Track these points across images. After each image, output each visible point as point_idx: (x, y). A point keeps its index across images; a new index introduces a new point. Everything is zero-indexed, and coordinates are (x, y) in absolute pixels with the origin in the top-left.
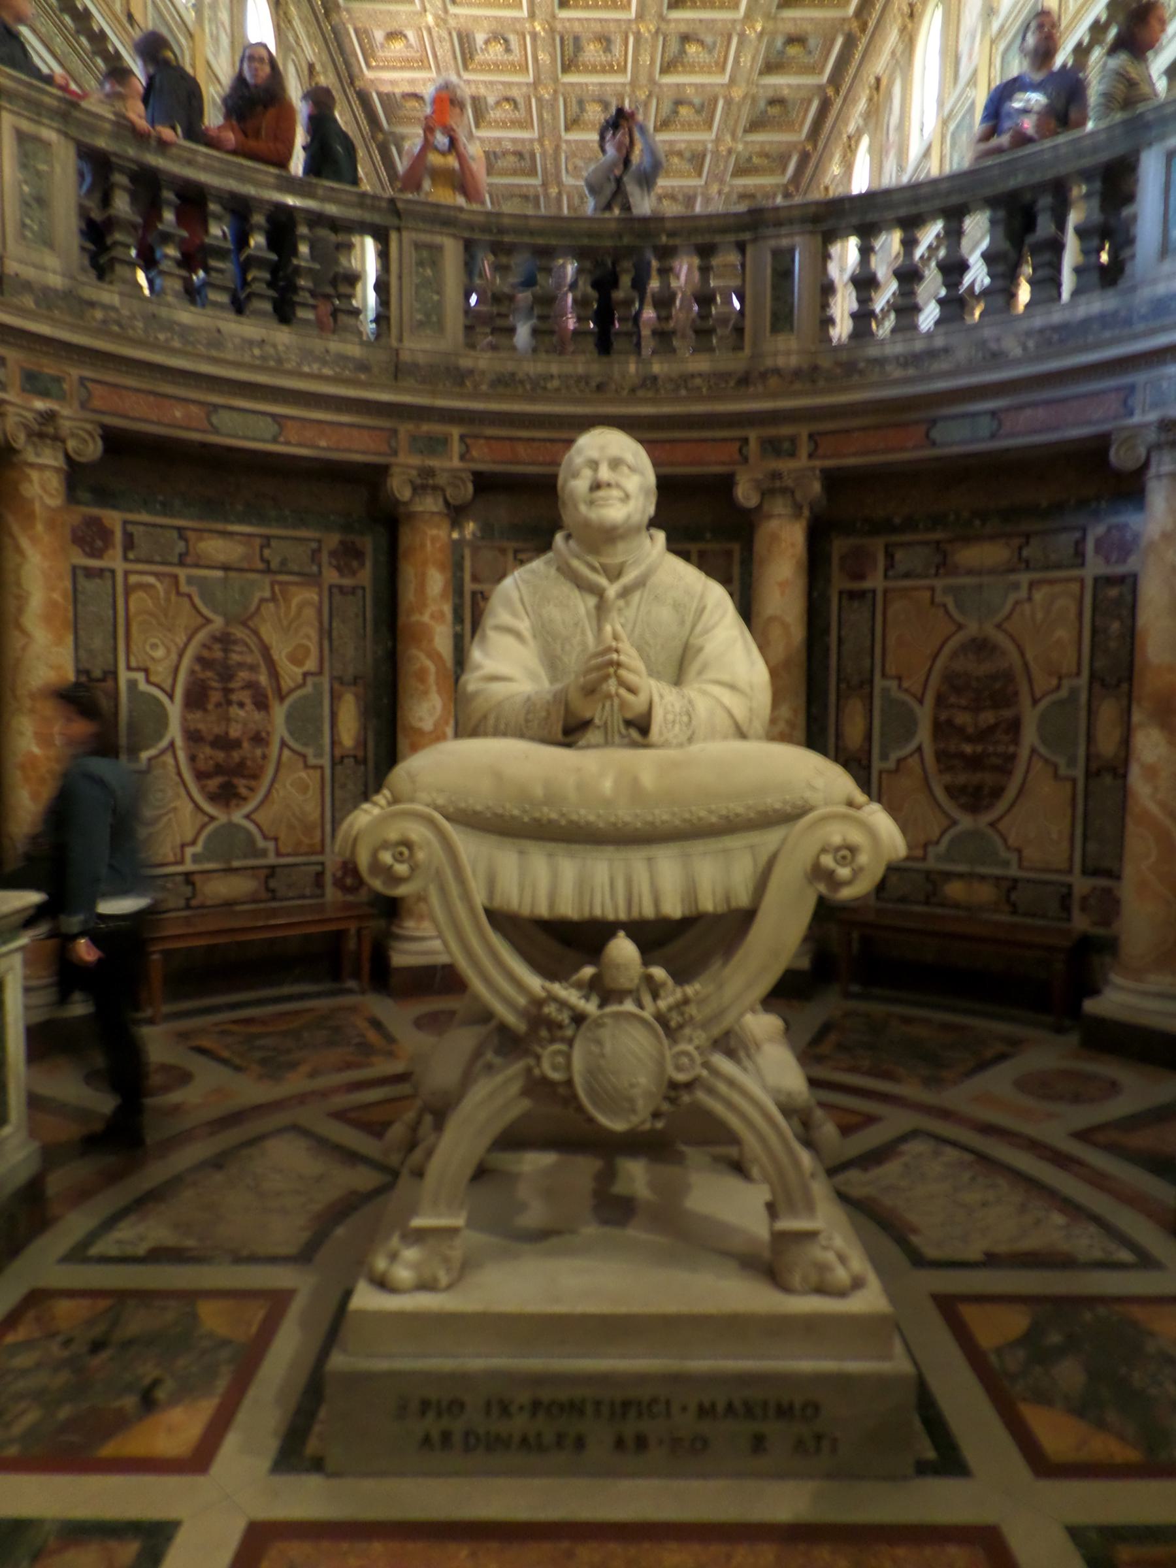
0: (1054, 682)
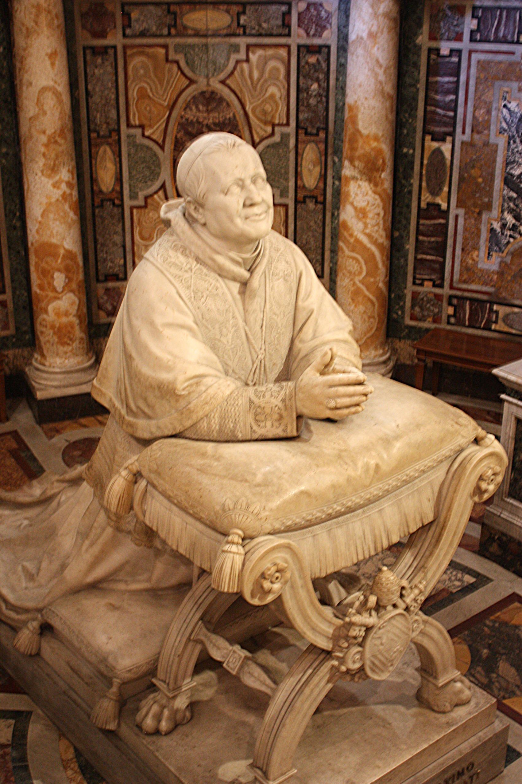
0: (269, 129)
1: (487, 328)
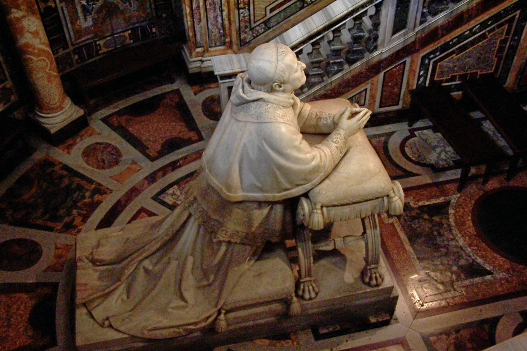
1: (98, 54)
